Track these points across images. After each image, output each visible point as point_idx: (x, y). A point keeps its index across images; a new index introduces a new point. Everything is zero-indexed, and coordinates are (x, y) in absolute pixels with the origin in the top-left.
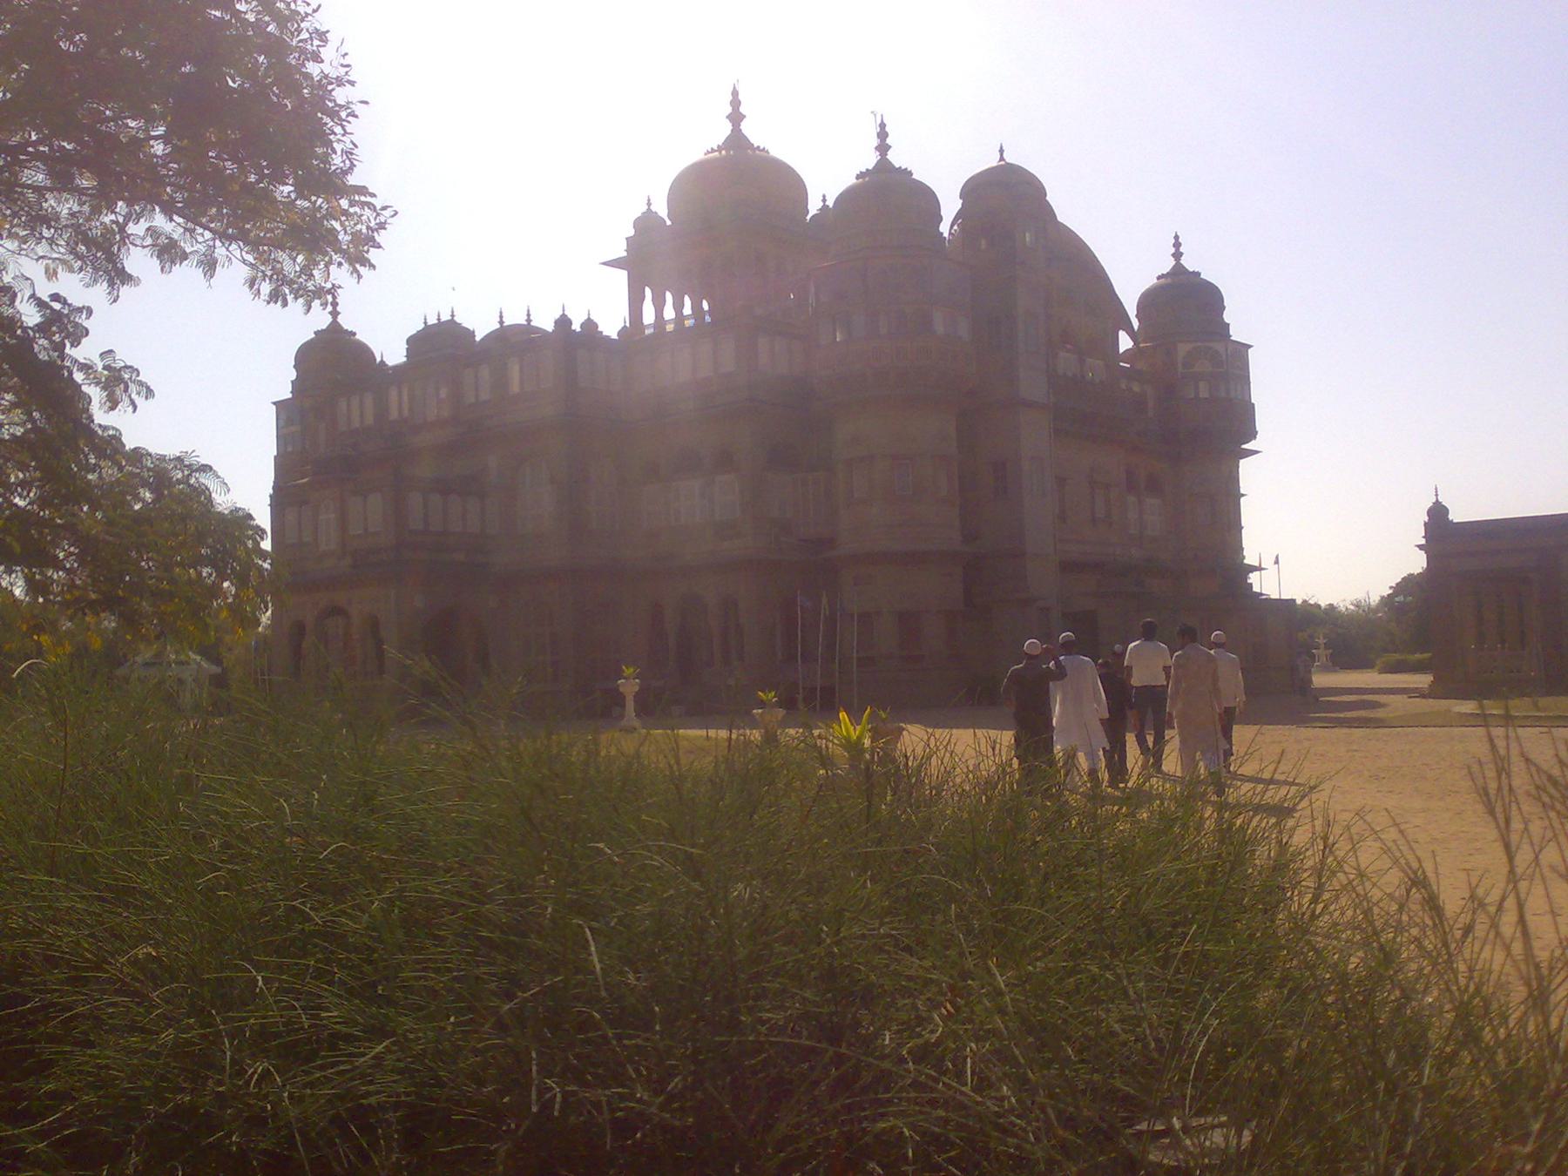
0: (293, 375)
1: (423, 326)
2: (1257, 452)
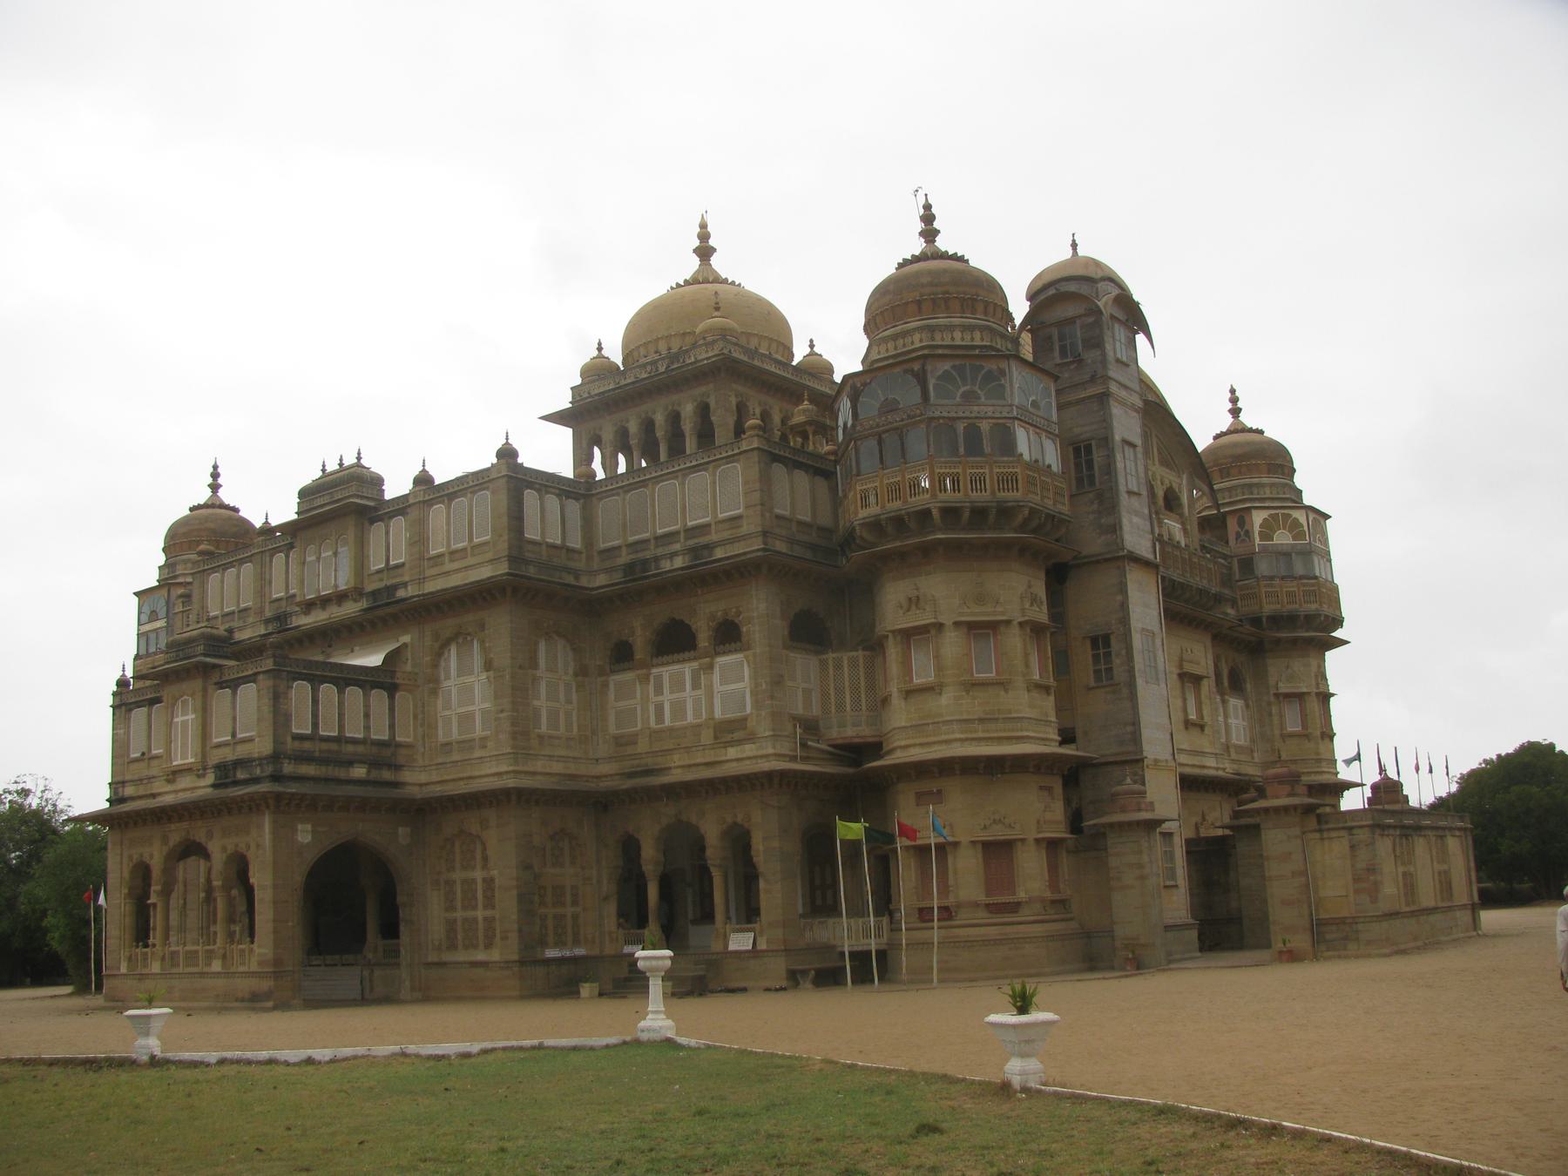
0: (161, 559)
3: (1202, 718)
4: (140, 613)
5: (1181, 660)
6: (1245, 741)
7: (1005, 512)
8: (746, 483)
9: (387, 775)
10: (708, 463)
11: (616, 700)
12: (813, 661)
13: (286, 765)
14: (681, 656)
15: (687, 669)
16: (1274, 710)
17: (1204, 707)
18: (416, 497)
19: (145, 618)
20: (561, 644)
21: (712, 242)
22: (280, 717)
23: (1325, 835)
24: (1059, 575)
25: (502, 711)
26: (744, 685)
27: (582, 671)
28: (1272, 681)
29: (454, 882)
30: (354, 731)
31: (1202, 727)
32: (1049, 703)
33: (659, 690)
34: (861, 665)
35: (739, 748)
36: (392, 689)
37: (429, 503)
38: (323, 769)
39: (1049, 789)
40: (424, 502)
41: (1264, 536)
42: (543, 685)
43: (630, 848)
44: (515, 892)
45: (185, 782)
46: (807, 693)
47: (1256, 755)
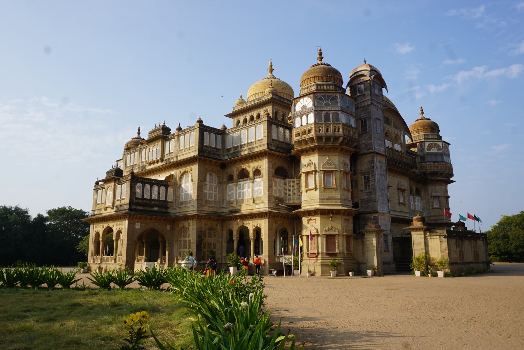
2: (454, 181)
3: (405, 202)
5: (398, 185)
6: (421, 210)
7: (336, 139)
8: (264, 130)
10: (254, 124)
11: (229, 191)
13: (133, 206)
14: (246, 179)
16: (430, 201)
17: (405, 199)
18: (177, 134)
20: (214, 175)
21: (273, 67)
23: (432, 237)
24: (355, 158)
25: (195, 193)
27: (220, 183)
28: (430, 192)
29: (181, 241)
30: (155, 197)
32: (349, 195)
33: (240, 189)
34: (296, 182)
35: (259, 205)
36: (167, 187)
38: (145, 208)
39: (348, 220)
40: (179, 135)
42: (208, 186)
43: (231, 232)
44: (195, 244)
45: (109, 210)
46: (280, 191)
47: (424, 214)
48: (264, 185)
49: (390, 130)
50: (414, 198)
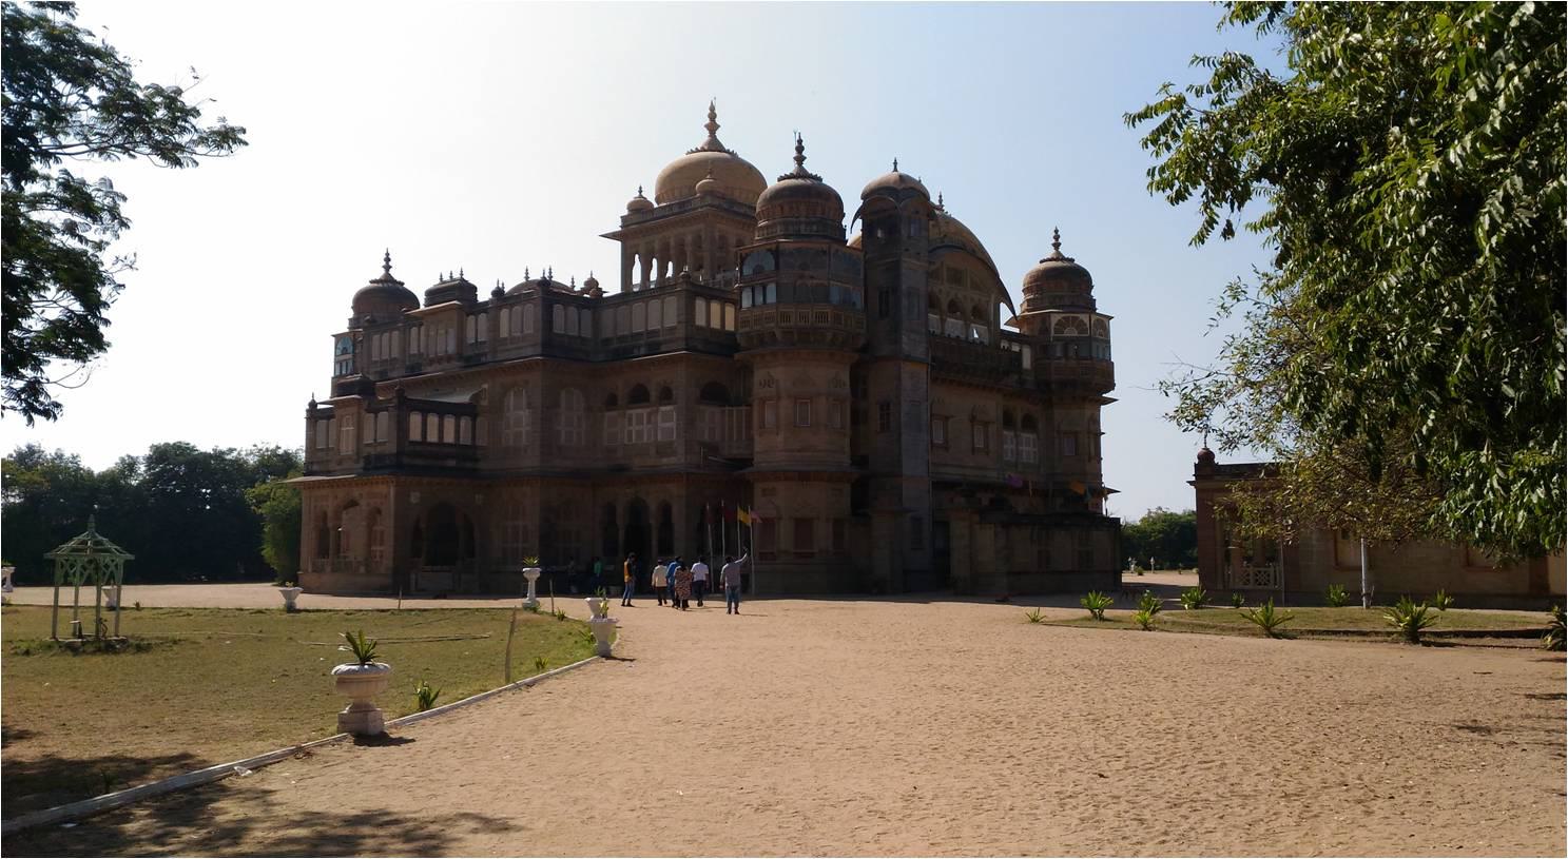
0: (351, 314)
1: (438, 282)
4: (336, 348)
9: (469, 465)
12: (717, 410)
15: (644, 412)
19: (339, 352)
22: (402, 428)
26: (672, 425)
31: (987, 453)
33: (630, 424)
37: (500, 308)
41: (1056, 331)
48: (678, 420)
49: (960, 296)
50: (1016, 436)
